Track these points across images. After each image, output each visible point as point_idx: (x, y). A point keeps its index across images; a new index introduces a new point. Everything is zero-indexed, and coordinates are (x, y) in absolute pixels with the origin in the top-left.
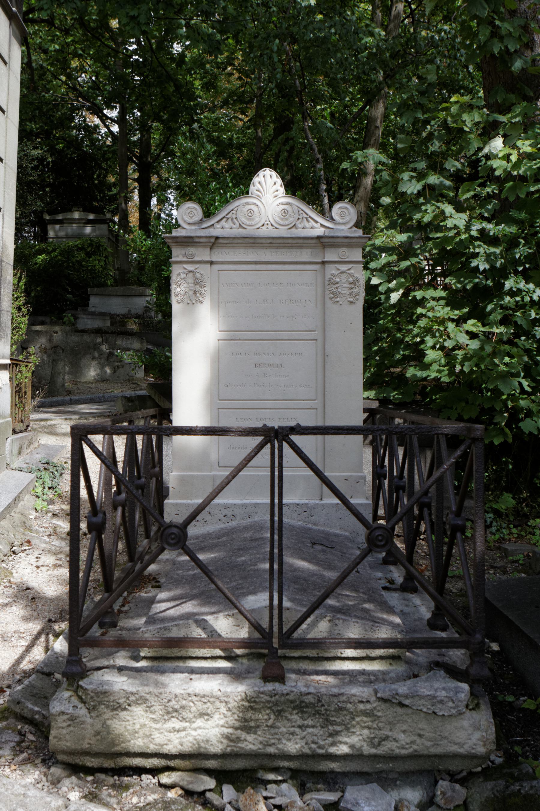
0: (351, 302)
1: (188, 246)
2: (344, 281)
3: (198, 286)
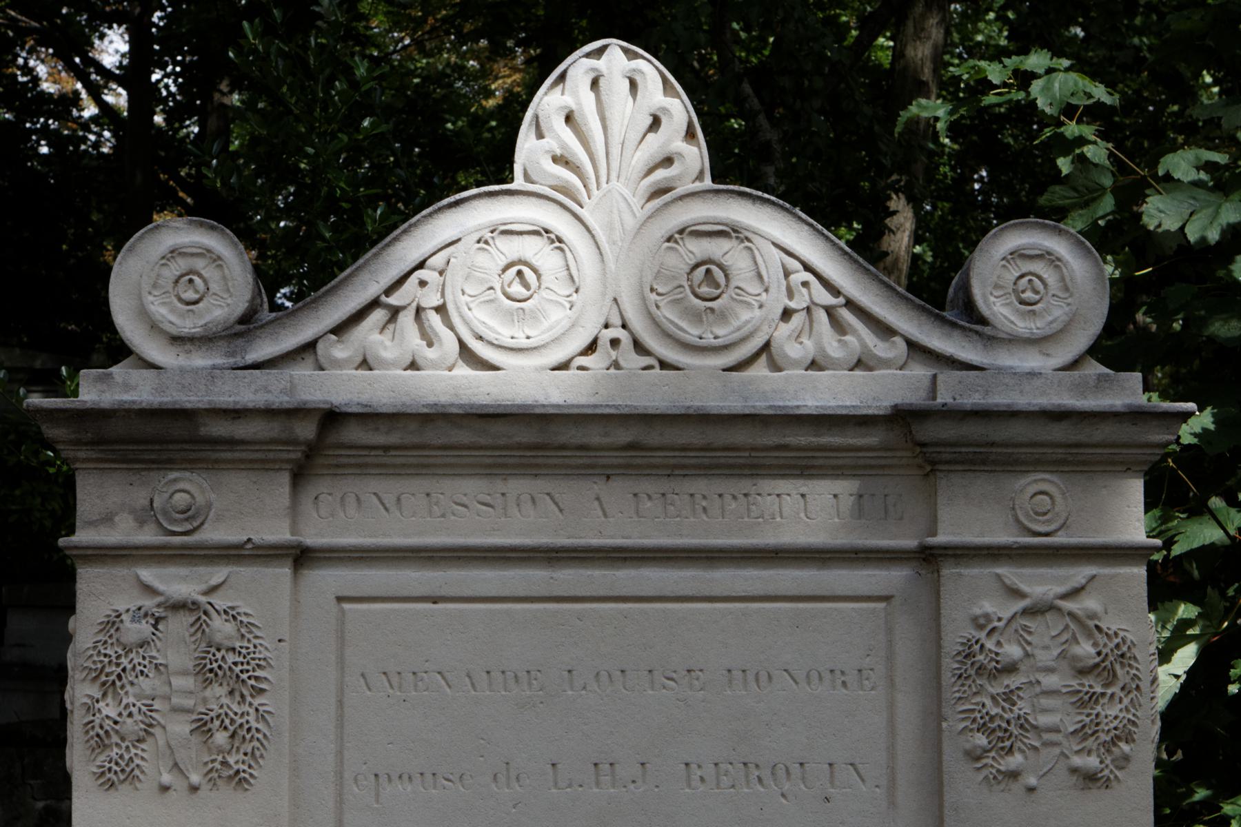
0: (1090, 778)
1: (166, 464)
2: (1044, 657)
3: (218, 691)
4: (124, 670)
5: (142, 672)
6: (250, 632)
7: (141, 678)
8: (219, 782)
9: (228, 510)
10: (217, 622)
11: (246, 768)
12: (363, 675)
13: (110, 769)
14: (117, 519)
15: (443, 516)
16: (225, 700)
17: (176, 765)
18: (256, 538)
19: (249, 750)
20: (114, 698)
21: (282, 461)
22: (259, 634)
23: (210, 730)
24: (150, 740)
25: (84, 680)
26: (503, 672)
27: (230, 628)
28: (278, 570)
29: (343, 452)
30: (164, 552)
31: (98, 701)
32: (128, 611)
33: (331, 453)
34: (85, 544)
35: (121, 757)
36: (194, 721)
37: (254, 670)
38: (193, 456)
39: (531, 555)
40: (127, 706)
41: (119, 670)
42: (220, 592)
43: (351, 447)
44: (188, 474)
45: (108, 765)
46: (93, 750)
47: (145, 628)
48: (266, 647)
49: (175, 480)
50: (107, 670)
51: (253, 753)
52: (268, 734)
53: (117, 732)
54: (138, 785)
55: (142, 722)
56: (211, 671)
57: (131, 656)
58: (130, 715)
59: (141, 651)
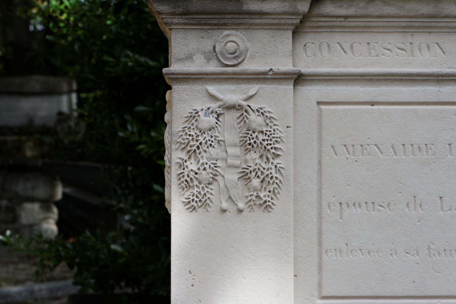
1: (223, 26)
3: (254, 155)
4: (201, 144)
5: (211, 145)
6: (272, 122)
7: (210, 148)
8: (254, 207)
9: (257, 53)
10: (253, 116)
11: (270, 199)
12: (332, 147)
13: (193, 200)
14: (194, 57)
15: (377, 56)
16: (258, 161)
17: (230, 197)
18: (275, 69)
19: (272, 189)
20: (195, 160)
21: (289, 24)
22: (276, 123)
23: (249, 178)
24: (215, 183)
25: (177, 149)
26: (412, 145)
27: (260, 120)
28: (286, 87)
29: (321, 19)
30: (222, 77)
31: (186, 161)
32: (202, 110)
33: (315, 20)
34: (178, 72)
35: (200, 193)
36: (240, 173)
37: (274, 144)
38: (238, 21)
39: (428, 78)
40: (203, 164)
41: (198, 144)
42: (254, 99)
43: (447, 17)
44: (234, 32)
45: (192, 198)
46: (183, 189)
47: (212, 120)
48: (280, 131)
49: (228, 35)
50: (191, 143)
51: (274, 191)
52: (282, 180)
53: (197, 179)
54: (209, 209)
55: (211, 173)
56: (250, 144)
57: (204, 136)
58: (205, 169)
59: (210, 133)
